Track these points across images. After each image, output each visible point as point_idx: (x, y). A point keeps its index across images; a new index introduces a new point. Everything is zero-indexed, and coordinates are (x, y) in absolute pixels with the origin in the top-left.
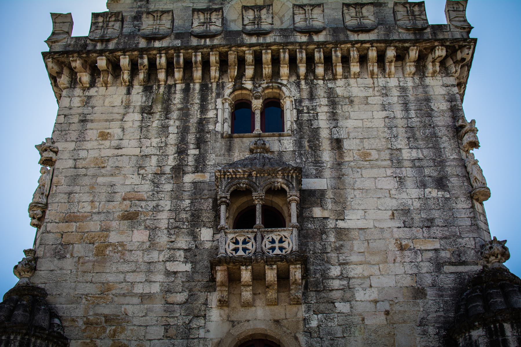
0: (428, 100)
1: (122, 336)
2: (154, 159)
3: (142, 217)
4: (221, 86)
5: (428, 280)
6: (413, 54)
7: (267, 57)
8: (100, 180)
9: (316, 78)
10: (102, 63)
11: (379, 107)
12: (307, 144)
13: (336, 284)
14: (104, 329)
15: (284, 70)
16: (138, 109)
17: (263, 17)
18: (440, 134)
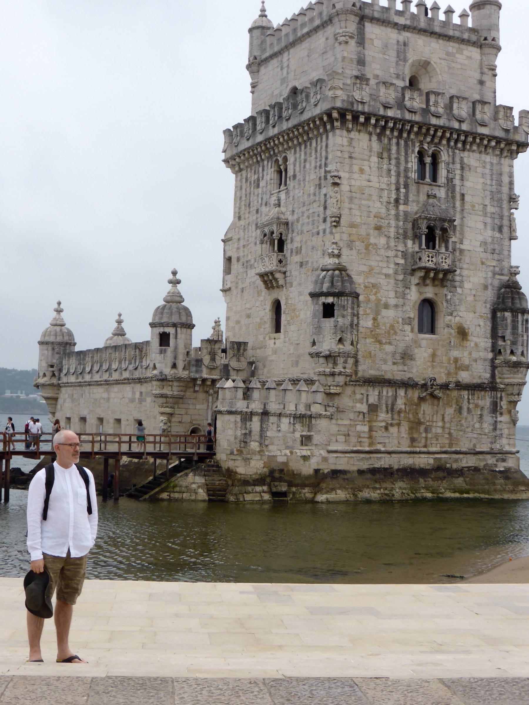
0: (501, 174)
1: (379, 295)
2: (386, 192)
3: (383, 230)
4: (414, 146)
5: (490, 281)
6: (502, 146)
7: (439, 134)
8: (364, 202)
9: (456, 148)
10: (362, 119)
11: (480, 175)
12: (450, 195)
13: (458, 278)
14: (372, 290)
15: (444, 142)
16: (376, 154)
17: (439, 101)
18: (503, 198)
